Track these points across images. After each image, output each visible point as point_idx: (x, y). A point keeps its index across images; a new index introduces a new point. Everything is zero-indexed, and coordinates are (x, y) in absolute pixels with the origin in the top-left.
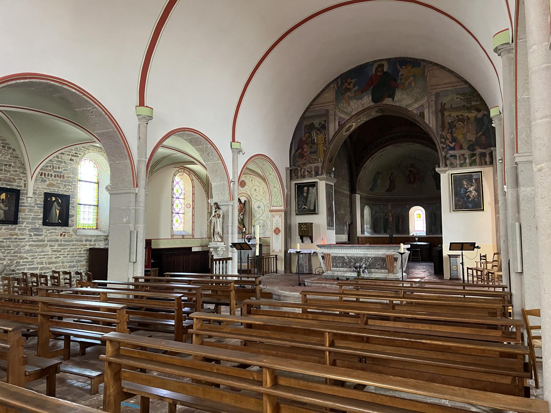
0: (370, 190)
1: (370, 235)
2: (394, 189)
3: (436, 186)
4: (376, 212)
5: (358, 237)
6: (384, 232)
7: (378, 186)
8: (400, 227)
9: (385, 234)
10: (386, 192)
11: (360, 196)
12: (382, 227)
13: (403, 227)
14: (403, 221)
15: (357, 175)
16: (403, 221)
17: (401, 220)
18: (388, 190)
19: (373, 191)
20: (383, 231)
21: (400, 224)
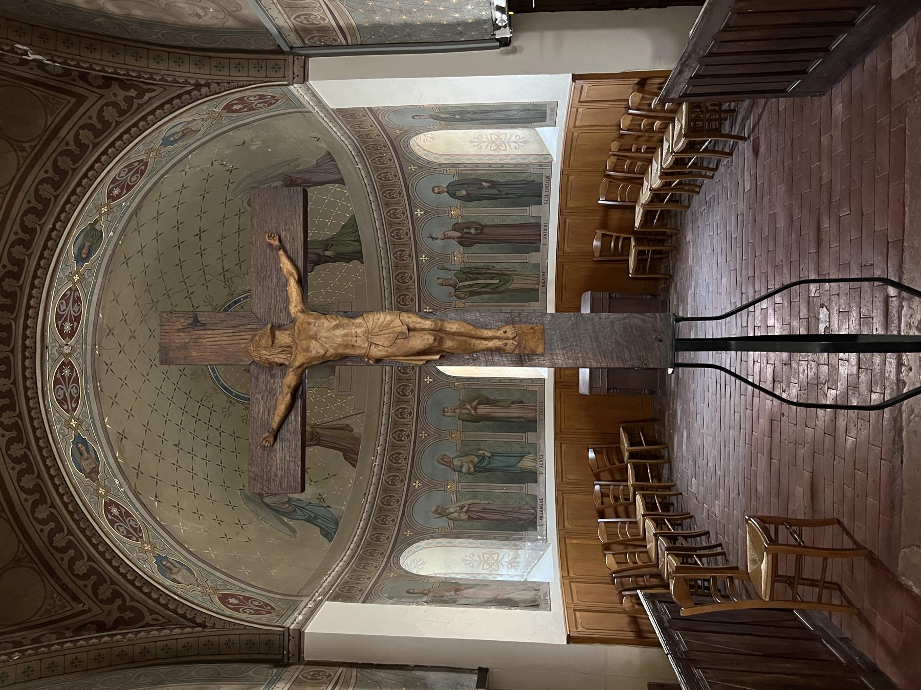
0: (328, 535)
1: (551, 546)
2: (347, 428)
3: (348, 261)
4: (441, 512)
5: (570, 639)
6: (535, 481)
7: (320, 498)
8: (515, 412)
9: (541, 478)
10: (354, 466)
11: (335, 598)
12: (513, 488)
13: (513, 403)
14: (488, 402)
15: (192, 620)
16: (488, 402)
17: (483, 410)
18: (351, 455)
19: (337, 524)
20: (530, 487)
21: (499, 412)
